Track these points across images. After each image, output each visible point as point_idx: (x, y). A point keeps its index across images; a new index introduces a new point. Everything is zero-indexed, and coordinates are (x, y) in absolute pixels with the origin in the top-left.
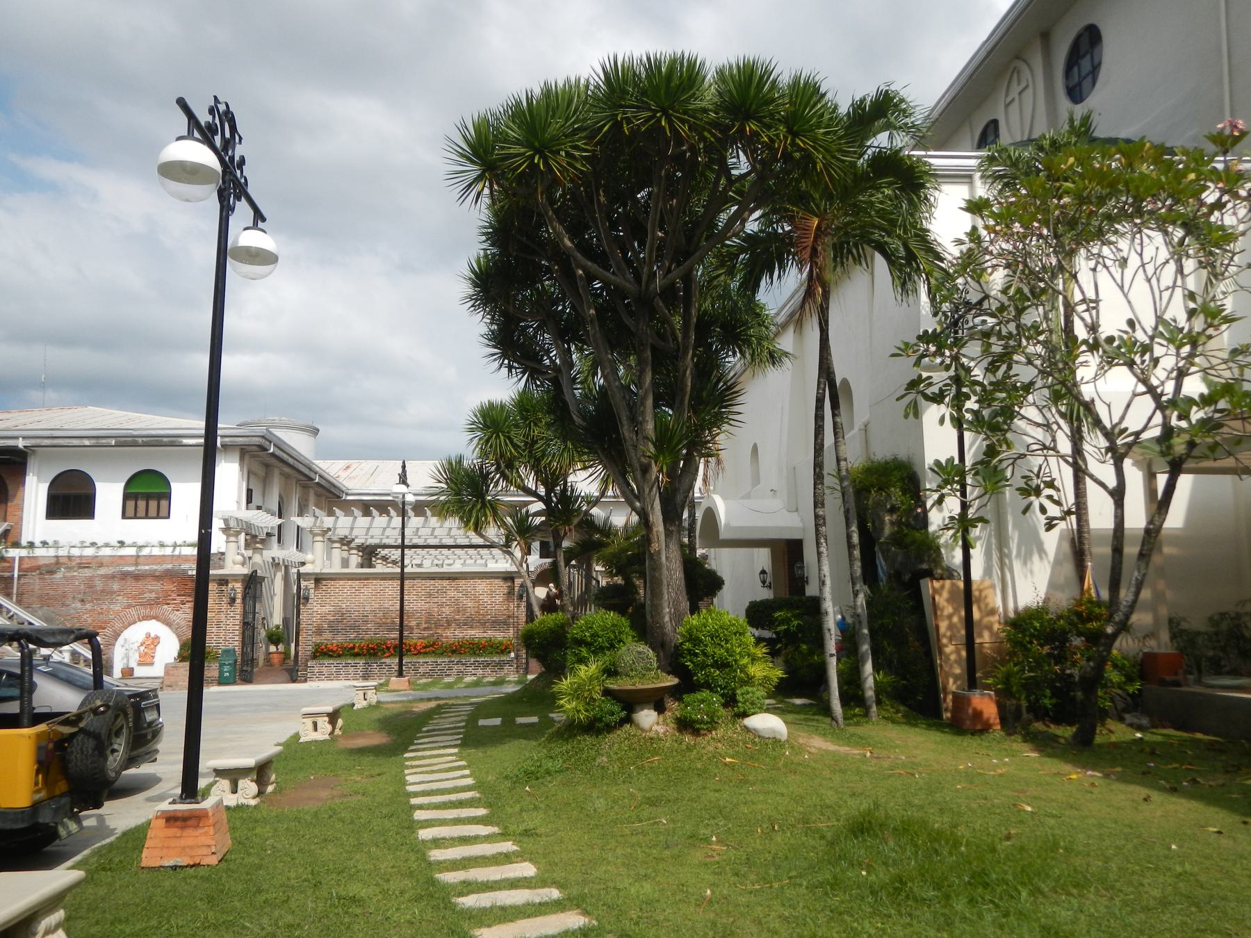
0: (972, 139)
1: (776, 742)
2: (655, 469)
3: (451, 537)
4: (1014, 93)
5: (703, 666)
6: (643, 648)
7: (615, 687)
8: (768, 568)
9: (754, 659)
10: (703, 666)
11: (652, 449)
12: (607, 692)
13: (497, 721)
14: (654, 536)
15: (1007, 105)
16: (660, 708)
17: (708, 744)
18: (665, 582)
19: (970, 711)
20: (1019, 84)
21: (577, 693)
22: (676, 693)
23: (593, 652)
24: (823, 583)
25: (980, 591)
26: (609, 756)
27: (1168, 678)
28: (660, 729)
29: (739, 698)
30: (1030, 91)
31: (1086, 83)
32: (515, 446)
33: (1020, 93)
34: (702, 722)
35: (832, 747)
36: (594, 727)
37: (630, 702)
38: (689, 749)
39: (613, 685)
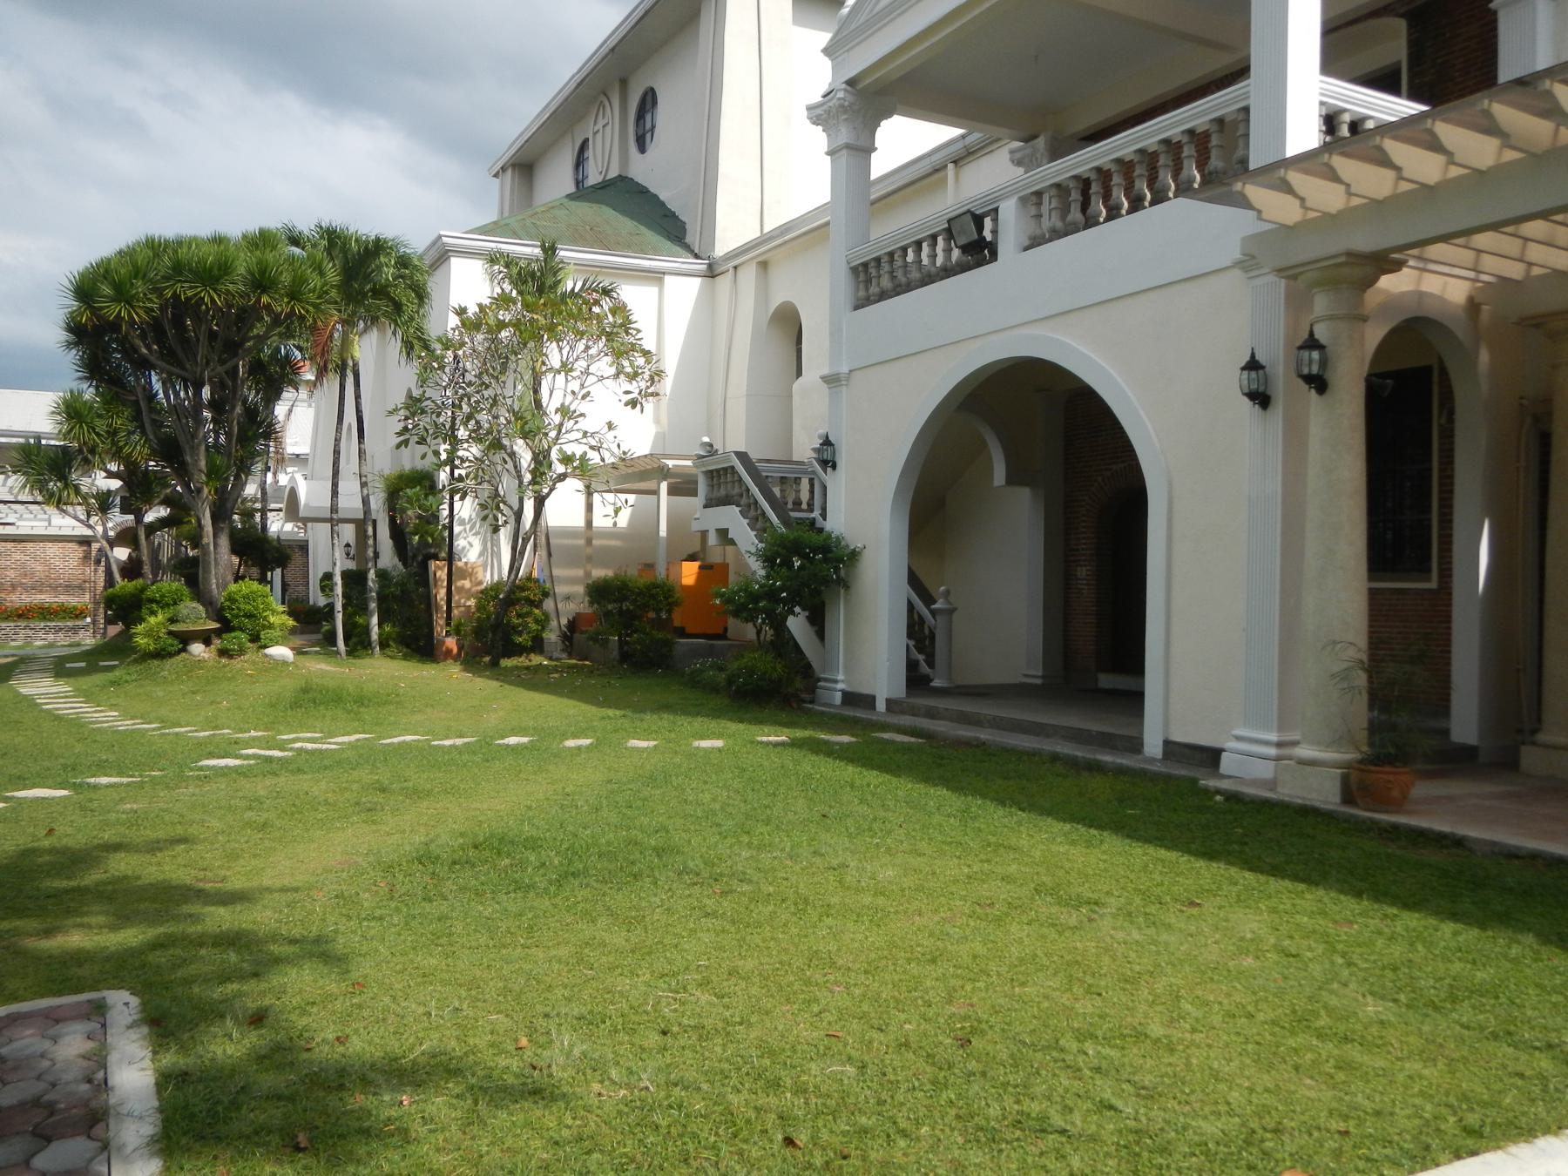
0: (573, 150)
1: (285, 663)
2: (206, 490)
3: (12, 494)
4: (601, 123)
5: (237, 616)
6: (195, 604)
7: (175, 629)
8: (352, 542)
9: (274, 612)
10: (237, 616)
11: (204, 478)
12: (170, 633)
13: (83, 664)
14: (205, 533)
15: (595, 133)
16: (207, 642)
17: (237, 663)
18: (213, 563)
19: (444, 649)
20: (603, 117)
21: (148, 634)
22: (218, 633)
23: (162, 607)
24: (335, 564)
25: (473, 569)
26: (169, 671)
27: (584, 629)
28: (206, 656)
29: (262, 636)
30: (609, 128)
31: (648, 136)
32: (98, 434)
33: (604, 127)
34: (233, 650)
35: (328, 668)
36: (160, 654)
37: (185, 639)
38: (224, 666)
39: (174, 628)
